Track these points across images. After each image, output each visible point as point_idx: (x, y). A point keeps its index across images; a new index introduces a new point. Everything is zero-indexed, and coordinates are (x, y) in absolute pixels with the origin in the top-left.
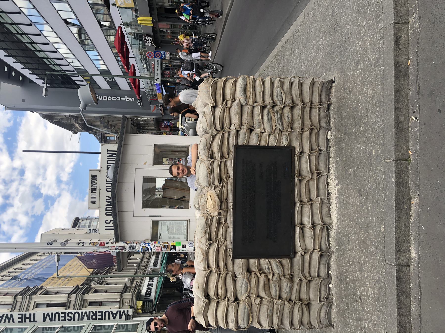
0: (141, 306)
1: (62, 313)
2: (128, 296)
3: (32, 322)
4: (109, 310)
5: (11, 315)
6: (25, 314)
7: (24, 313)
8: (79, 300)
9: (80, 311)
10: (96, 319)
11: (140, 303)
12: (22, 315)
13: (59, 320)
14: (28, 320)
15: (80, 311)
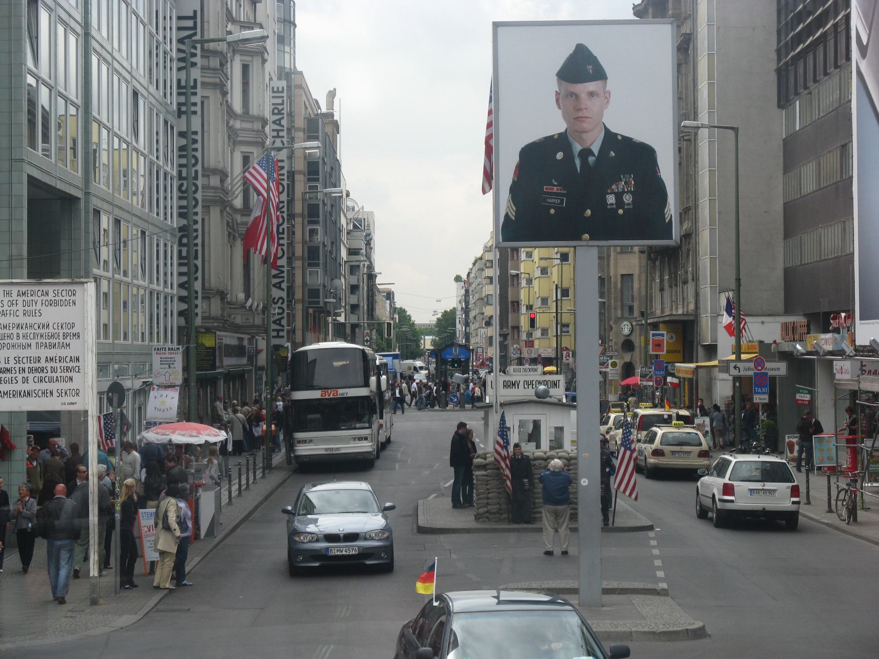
0: (203, 344)
1: (196, 172)
2: (216, 307)
3: (179, 109)
4: (199, 274)
5: (194, 64)
6: (195, 94)
7: (199, 90)
8: (210, 194)
9: (199, 209)
10: (181, 244)
11: (208, 342)
12: (195, 87)
13: (181, 166)
14: (182, 99)
15: (199, 209)
